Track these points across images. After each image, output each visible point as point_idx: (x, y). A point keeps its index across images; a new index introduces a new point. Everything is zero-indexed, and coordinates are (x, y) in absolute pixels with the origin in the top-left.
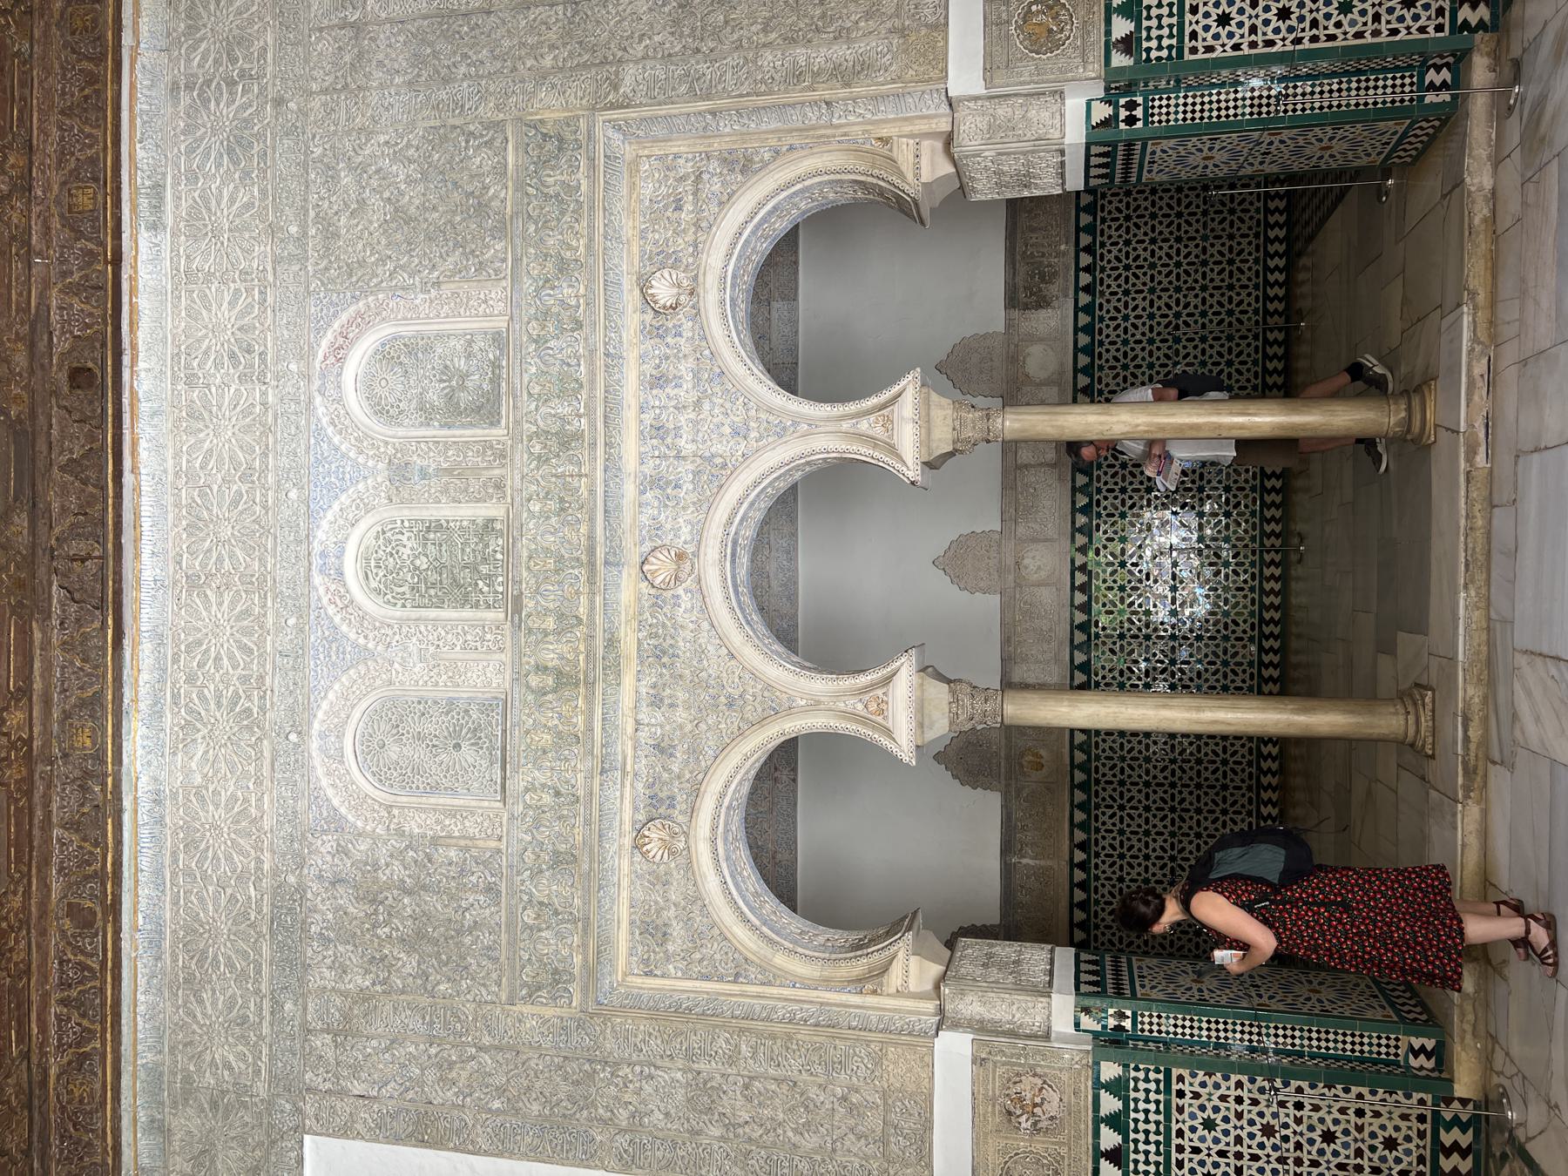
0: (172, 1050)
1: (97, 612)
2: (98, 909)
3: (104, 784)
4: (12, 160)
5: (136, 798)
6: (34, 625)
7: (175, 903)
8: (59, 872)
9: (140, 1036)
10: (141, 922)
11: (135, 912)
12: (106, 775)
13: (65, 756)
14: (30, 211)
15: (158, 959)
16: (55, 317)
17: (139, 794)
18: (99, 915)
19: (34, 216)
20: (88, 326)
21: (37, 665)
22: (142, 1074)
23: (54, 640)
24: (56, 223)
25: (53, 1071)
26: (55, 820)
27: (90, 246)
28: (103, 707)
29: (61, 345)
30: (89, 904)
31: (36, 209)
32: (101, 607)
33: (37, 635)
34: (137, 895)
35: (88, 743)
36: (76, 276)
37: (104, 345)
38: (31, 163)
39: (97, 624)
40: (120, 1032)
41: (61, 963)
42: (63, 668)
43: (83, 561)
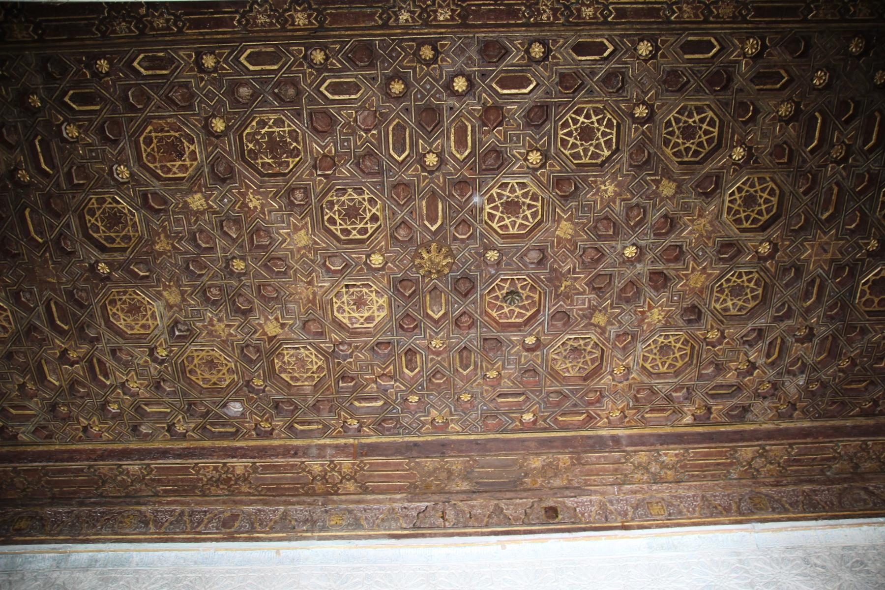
0: (137, 572)
1: (411, 526)
2: (233, 530)
3: (307, 531)
4: (669, 472)
5: (296, 548)
6: (404, 495)
7: (227, 572)
8: (259, 510)
9: (151, 553)
10: (220, 553)
11: (226, 550)
12: (313, 532)
13: (326, 512)
14: (643, 483)
15: (195, 563)
16: (585, 498)
17: (299, 550)
18: (228, 530)
19: (641, 485)
20: (583, 515)
21: (381, 497)
22: (127, 555)
23: (395, 505)
24: (639, 496)
25: (143, 508)
26: (290, 507)
27: (630, 514)
28: (354, 530)
29: (569, 502)
30: (236, 524)
31: (645, 486)
32: (415, 527)
33: (398, 496)
34: (236, 550)
35: (333, 523)
36: (611, 508)
37: (573, 523)
38: (670, 483)
39: (404, 526)
40: (156, 542)
41: (205, 512)
42: (379, 509)
43: (443, 517)
